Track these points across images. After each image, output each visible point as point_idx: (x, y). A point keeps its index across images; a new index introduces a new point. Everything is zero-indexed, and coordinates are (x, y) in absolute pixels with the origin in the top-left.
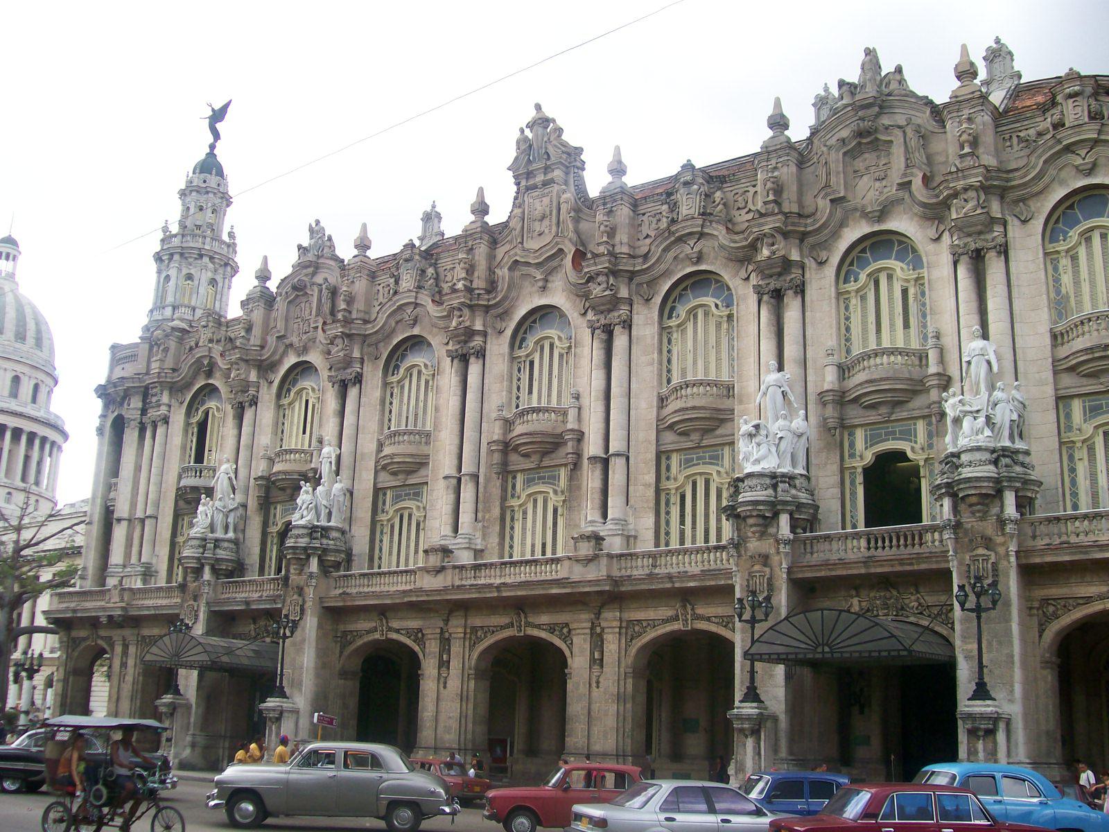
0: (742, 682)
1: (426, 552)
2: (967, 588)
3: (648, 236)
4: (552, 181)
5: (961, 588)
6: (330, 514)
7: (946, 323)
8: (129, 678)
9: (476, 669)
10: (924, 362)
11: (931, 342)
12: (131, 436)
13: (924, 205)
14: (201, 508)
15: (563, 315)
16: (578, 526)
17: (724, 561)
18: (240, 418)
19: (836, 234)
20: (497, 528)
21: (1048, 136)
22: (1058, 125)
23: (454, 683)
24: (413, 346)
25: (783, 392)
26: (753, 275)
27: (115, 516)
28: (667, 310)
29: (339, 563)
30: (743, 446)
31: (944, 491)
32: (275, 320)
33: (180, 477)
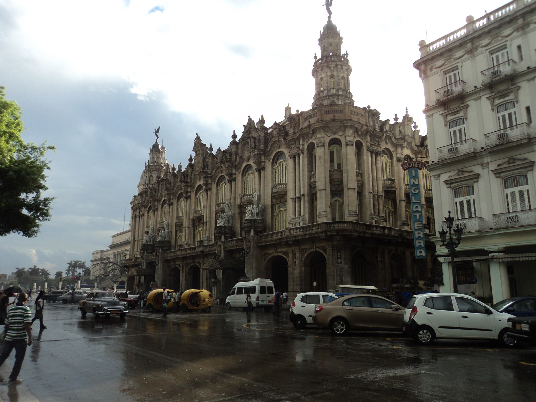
6: (165, 237)
12: (138, 219)
18: (154, 214)
19: (241, 166)
28: (218, 185)
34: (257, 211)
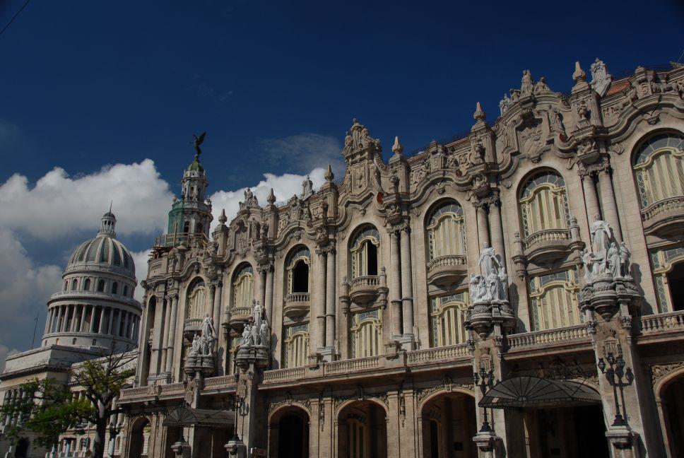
0: (481, 420)
1: (309, 357)
2: (605, 360)
3: (416, 182)
4: (364, 158)
5: (601, 360)
7: (578, 212)
8: (160, 434)
9: (339, 419)
10: (569, 236)
11: (572, 225)
12: (159, 307)
13: (562, 151)
14: (194, 341)
15: (374, 228)
16: (388, 339)
17: (465, 353)
19: (515, 172)
20: (346, 343)
21: (630, 105)
22: (635, 99)
23: (327, 427)
24: (299, 251)
25: (492, 258)
26: (472, 197)
27: (153, 348)
29: (266, 366)
30: (472, 289)
31: (585, 305)
32: (230, 241)
33: (184, 326)
34: (623, 261)
